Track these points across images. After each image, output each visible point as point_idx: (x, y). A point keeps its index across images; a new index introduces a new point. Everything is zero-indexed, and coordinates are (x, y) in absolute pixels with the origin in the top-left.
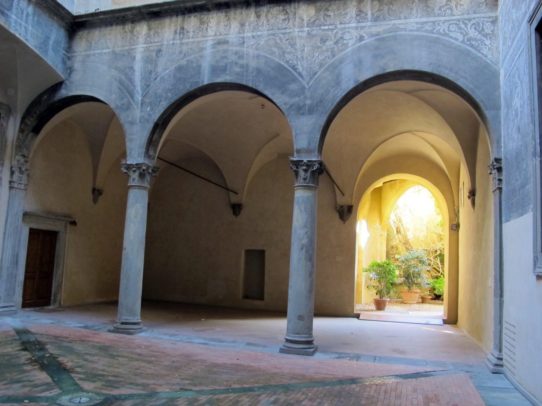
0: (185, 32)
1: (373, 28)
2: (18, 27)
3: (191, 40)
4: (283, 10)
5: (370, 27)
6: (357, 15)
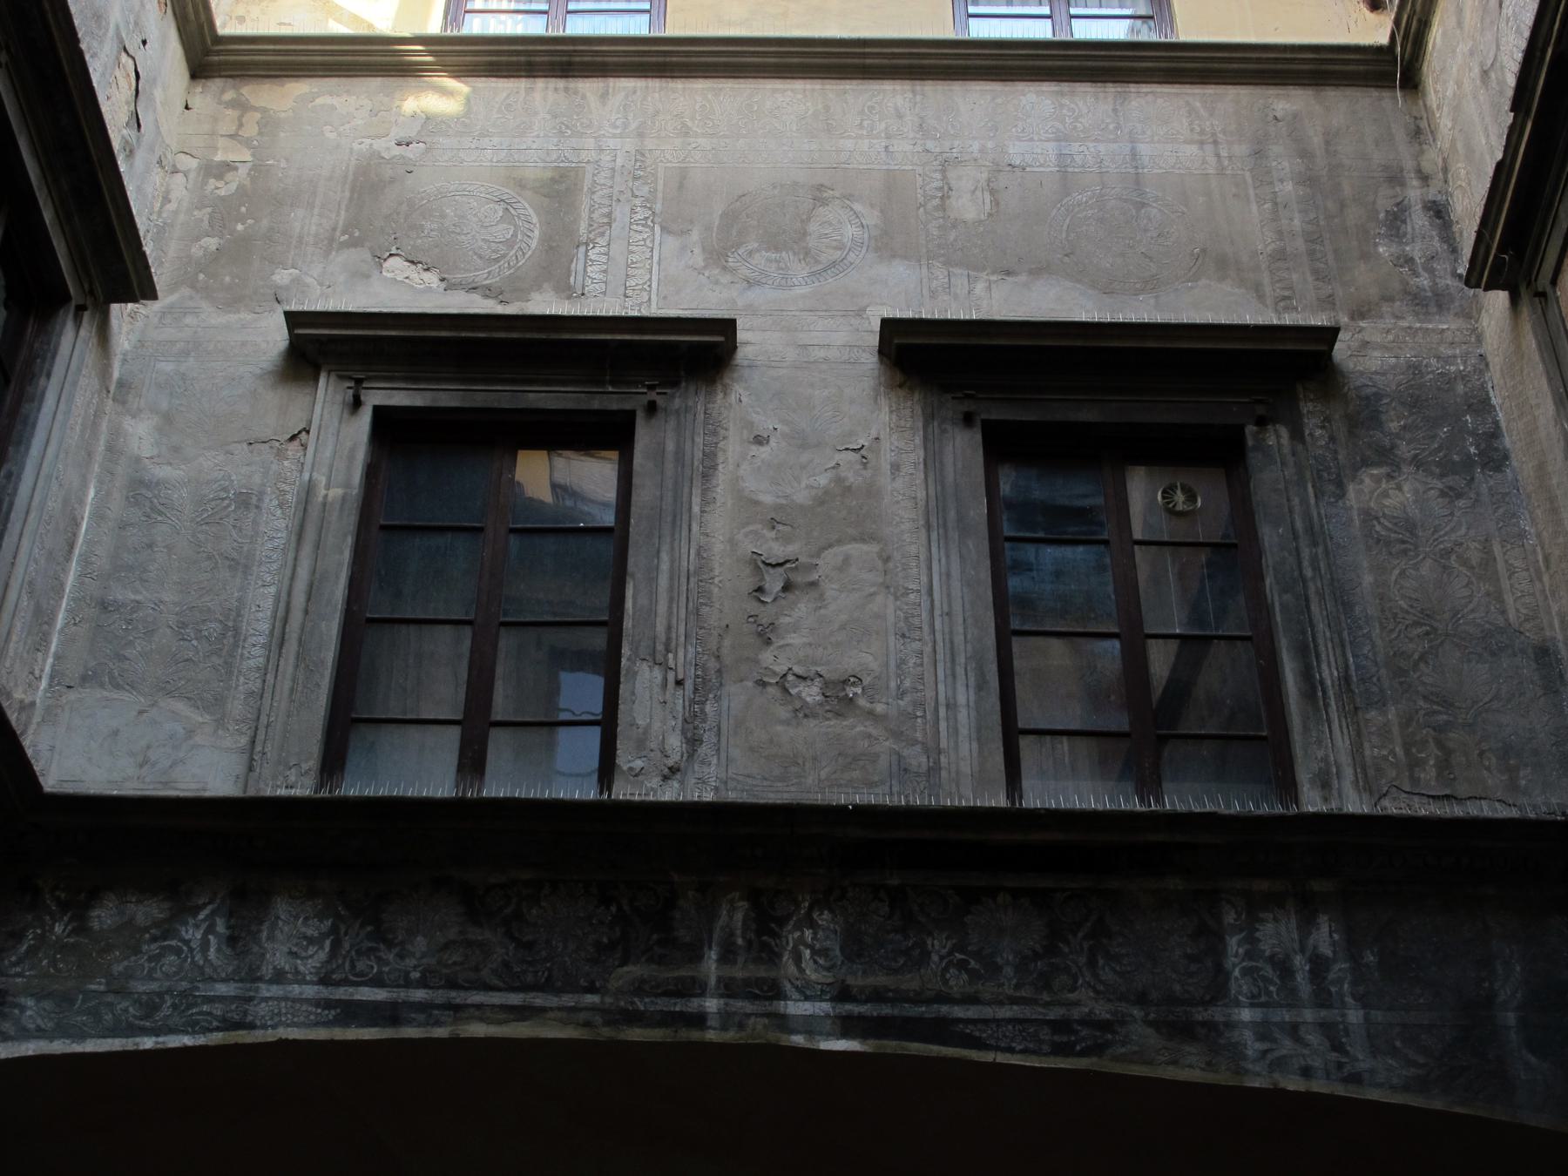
2: (1287, 1046)
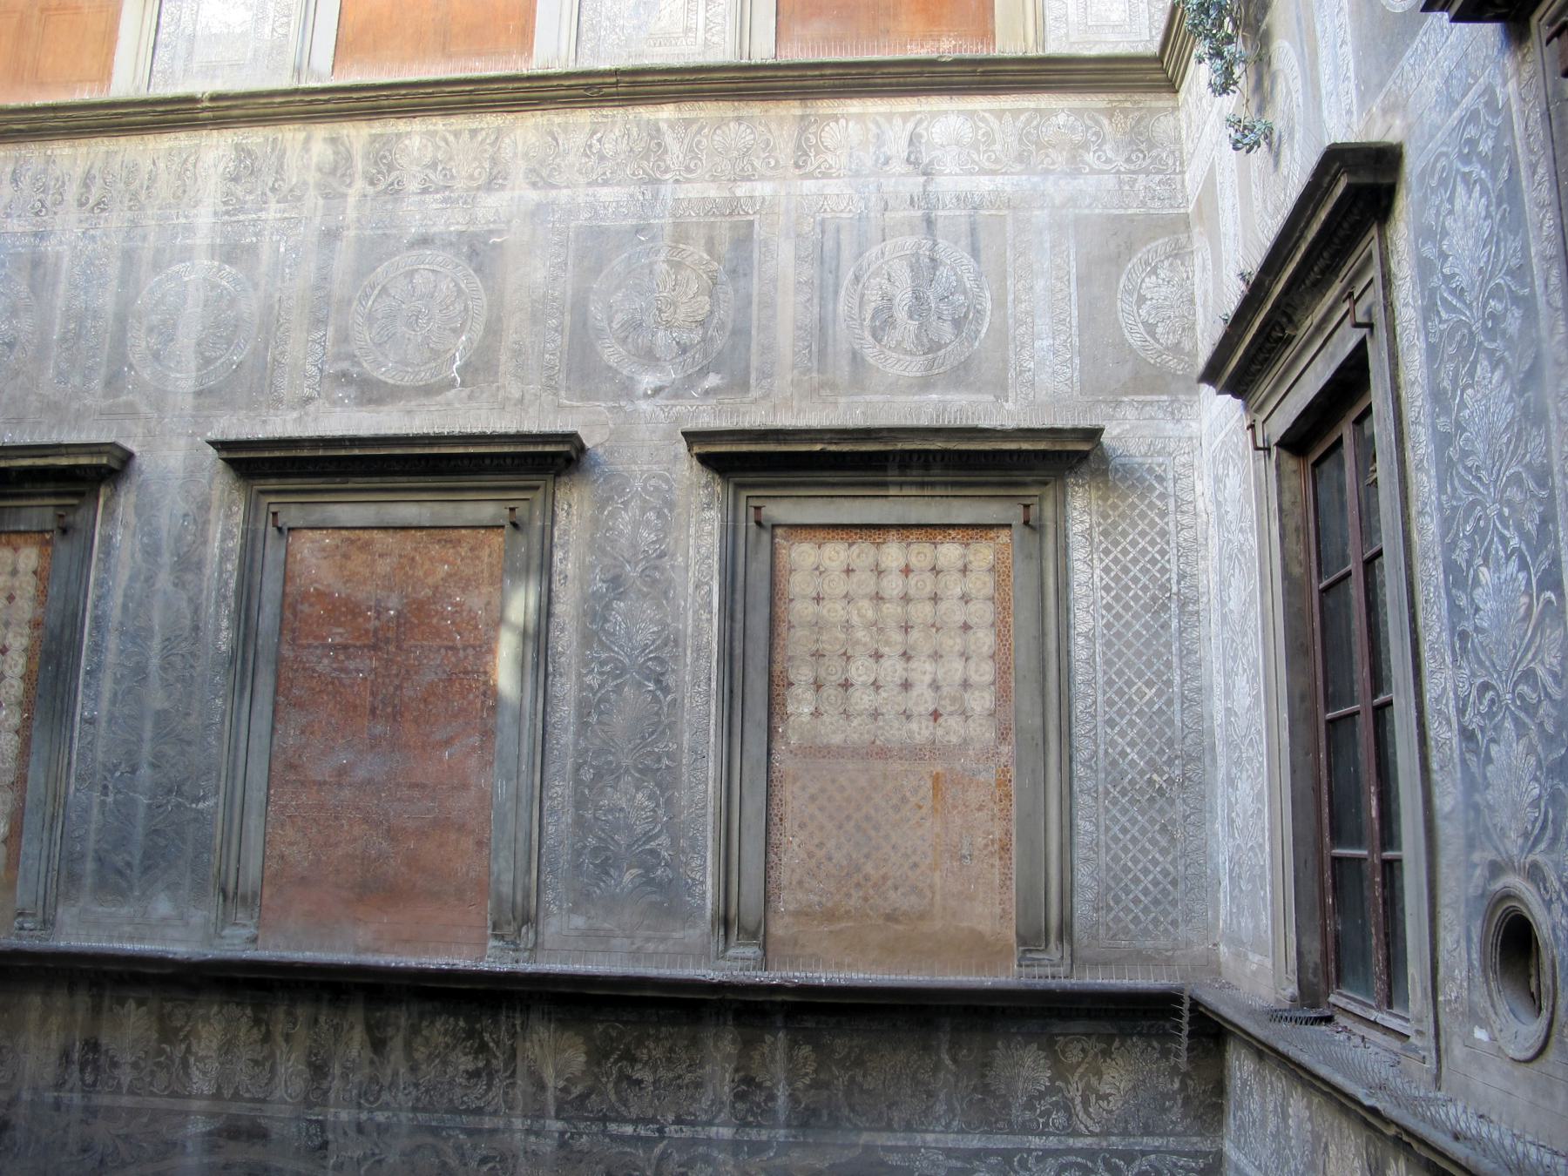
0: (103, 1060)
1: (795, 1154)
3: (126, 1101)
4: (471, 1034)
5: (785, 1147)
6: (740, 1096)
